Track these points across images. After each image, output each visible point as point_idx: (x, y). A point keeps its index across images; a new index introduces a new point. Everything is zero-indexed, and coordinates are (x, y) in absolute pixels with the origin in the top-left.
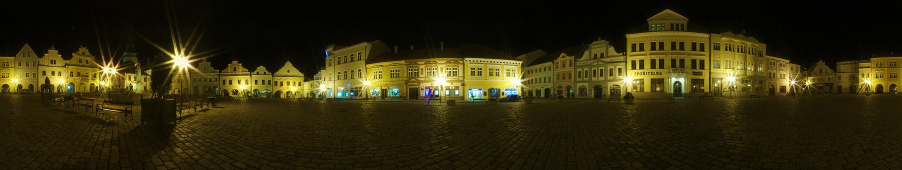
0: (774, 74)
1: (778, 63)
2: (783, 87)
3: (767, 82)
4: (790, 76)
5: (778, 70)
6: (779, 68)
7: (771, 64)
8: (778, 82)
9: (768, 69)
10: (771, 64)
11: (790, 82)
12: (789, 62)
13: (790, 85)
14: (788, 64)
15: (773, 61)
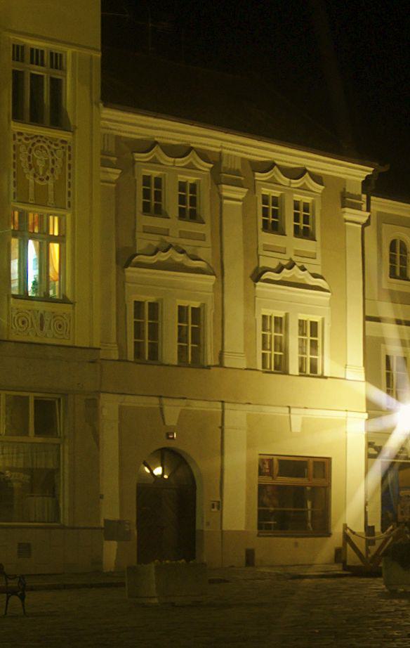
0: (192, 319)
1: (234, 194)
2: (294, 465)
3: (110, 406)
4: (372, 347)
5: (236, 273)
6: (251, 250)
7: (154, 207)
8: (236, 417)
9: (126, 258)
10: (154, 207)
11: (374, 410)
12: (369, 186)
13: (374, 449)
14: (346, 200)
15: (176, 173)
